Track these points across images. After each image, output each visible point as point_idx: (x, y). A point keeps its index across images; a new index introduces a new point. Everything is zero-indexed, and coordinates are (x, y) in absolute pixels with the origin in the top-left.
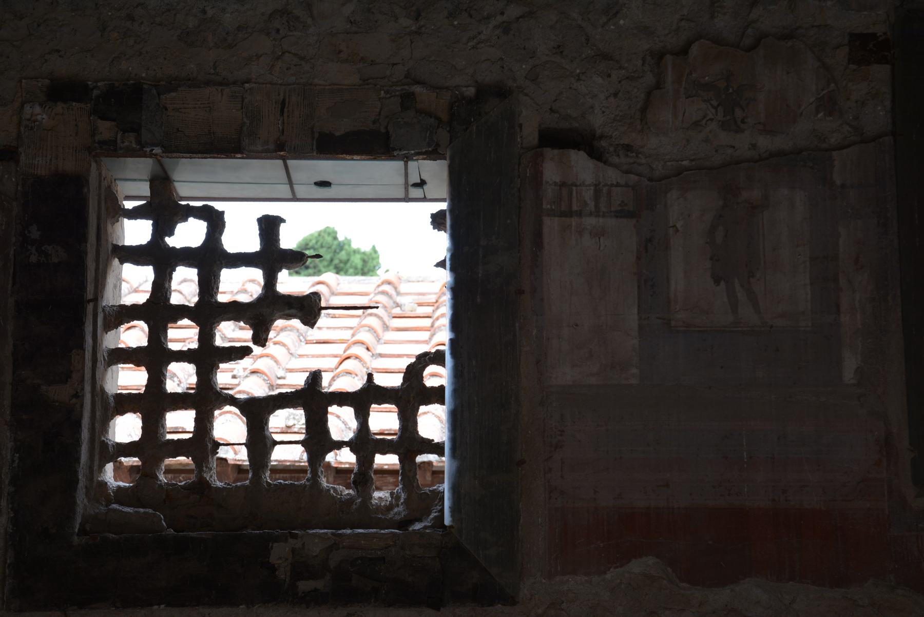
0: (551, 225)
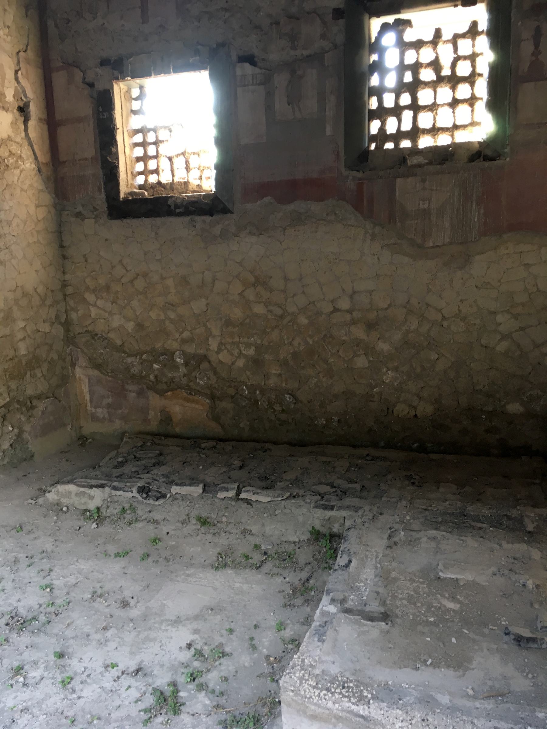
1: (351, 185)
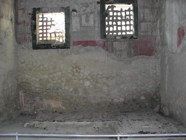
0: (73, 18)
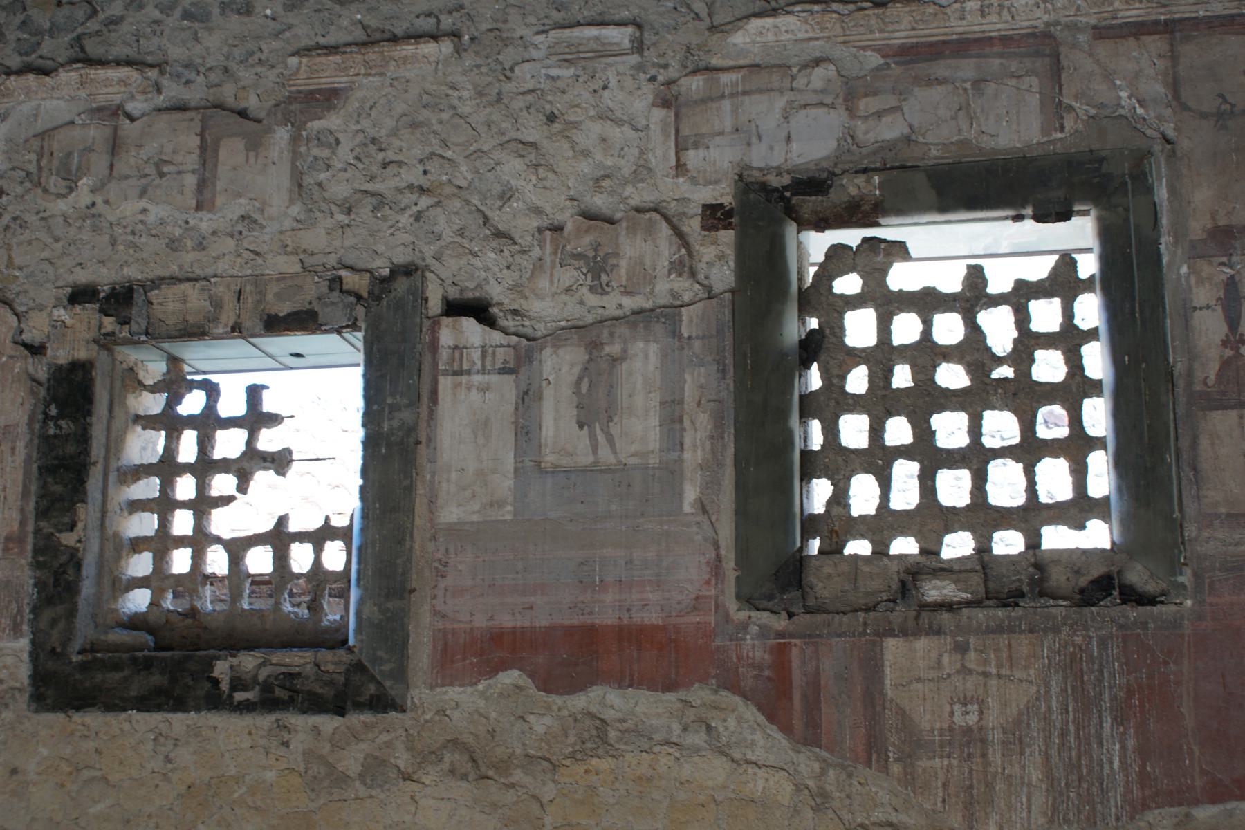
0: (445, 383)
1: (754, 649)
